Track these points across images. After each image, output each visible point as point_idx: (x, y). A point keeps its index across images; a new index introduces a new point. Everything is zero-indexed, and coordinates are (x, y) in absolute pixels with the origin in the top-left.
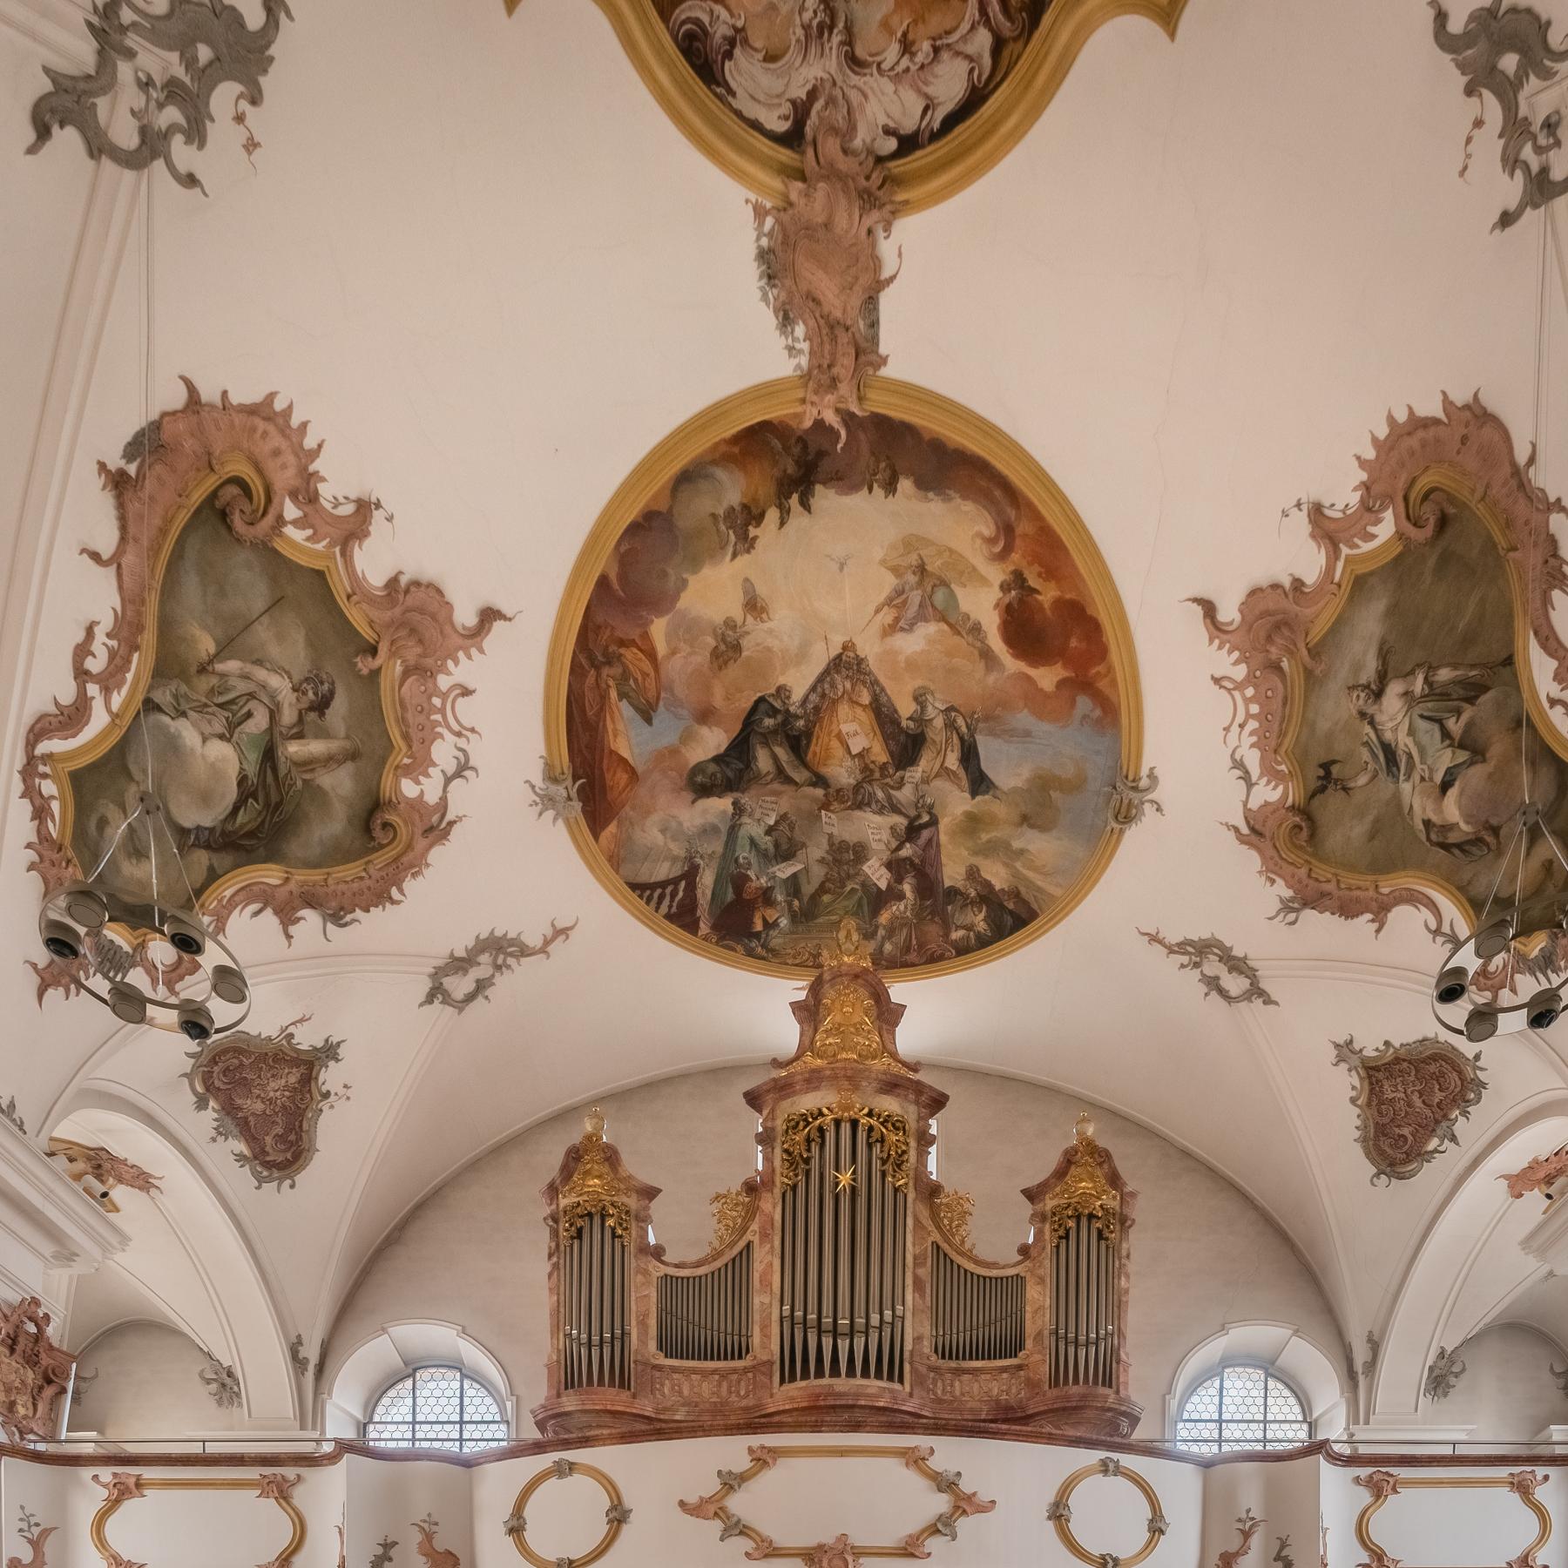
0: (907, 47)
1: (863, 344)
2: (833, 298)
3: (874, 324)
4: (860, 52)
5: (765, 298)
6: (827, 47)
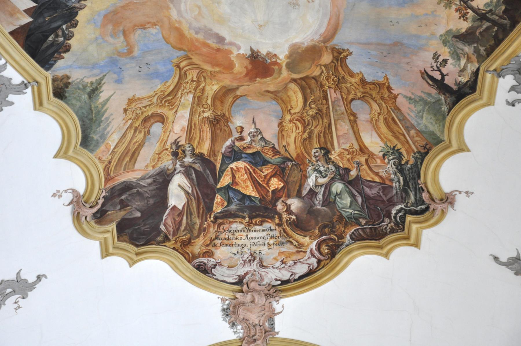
0: (283, 262)
1: (268, 329)
2: (254, 318)
3: (272, 324)
4: (264, 264)
5: (224, 320)
6: (252, 264)
